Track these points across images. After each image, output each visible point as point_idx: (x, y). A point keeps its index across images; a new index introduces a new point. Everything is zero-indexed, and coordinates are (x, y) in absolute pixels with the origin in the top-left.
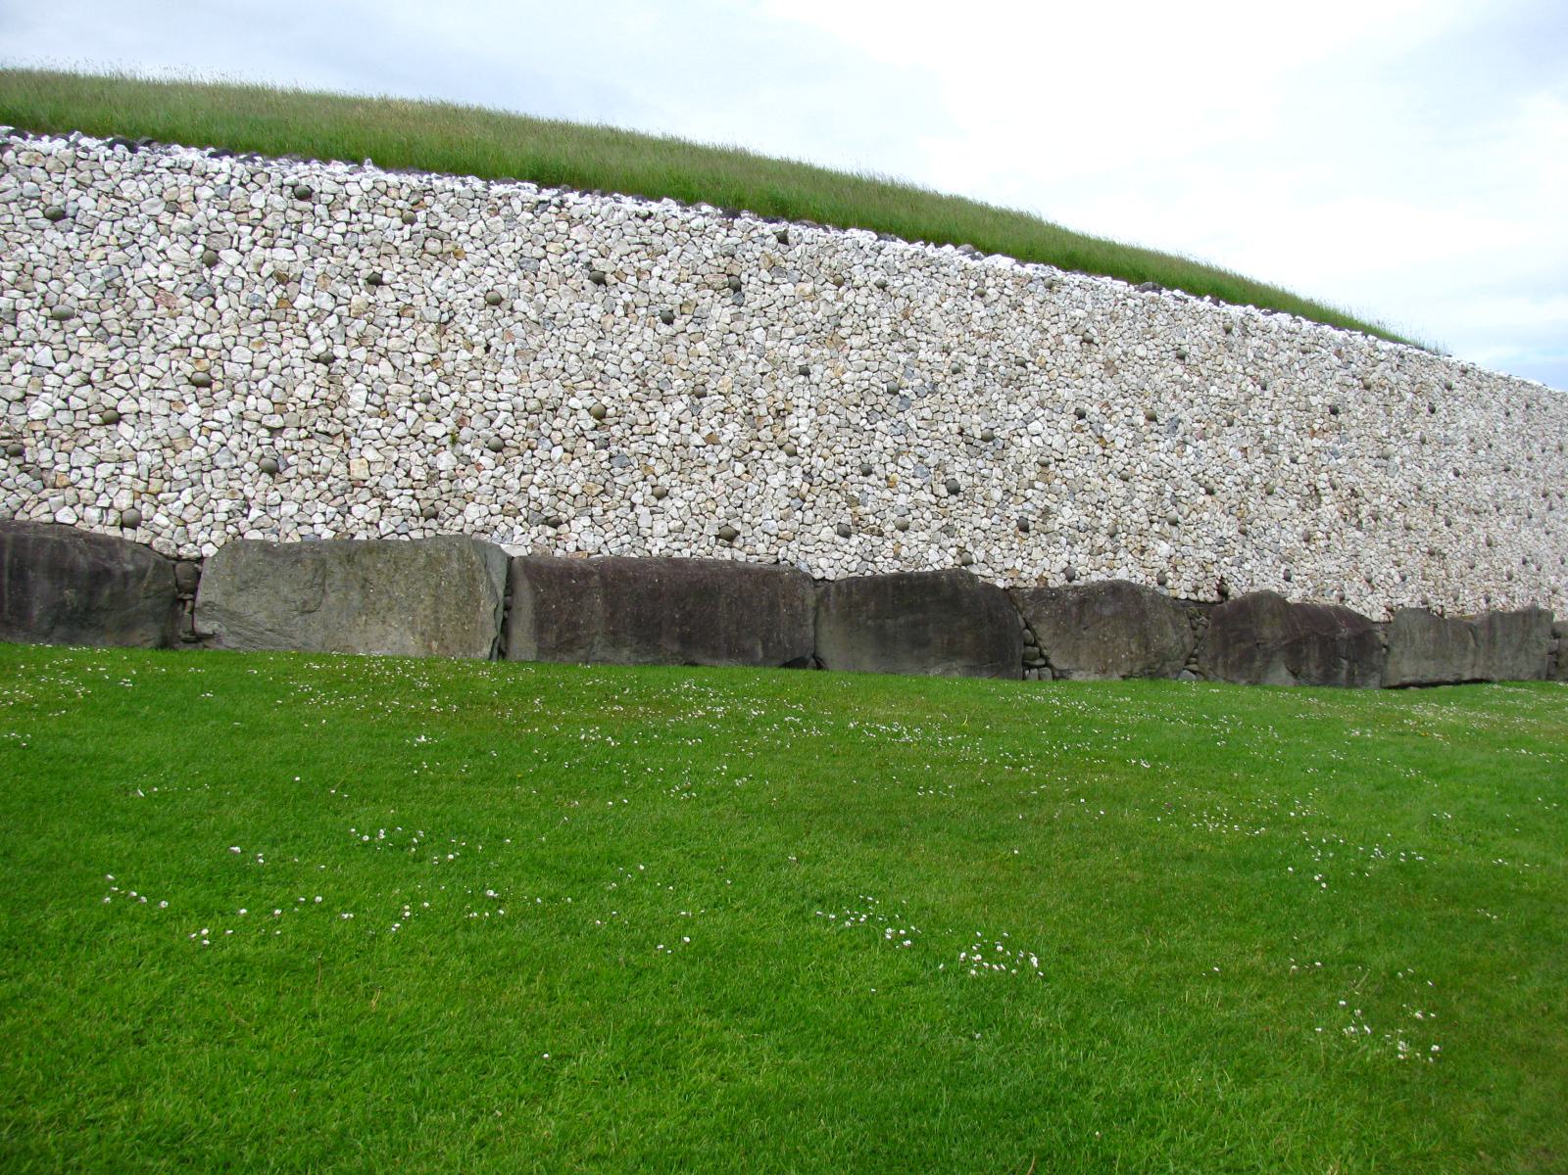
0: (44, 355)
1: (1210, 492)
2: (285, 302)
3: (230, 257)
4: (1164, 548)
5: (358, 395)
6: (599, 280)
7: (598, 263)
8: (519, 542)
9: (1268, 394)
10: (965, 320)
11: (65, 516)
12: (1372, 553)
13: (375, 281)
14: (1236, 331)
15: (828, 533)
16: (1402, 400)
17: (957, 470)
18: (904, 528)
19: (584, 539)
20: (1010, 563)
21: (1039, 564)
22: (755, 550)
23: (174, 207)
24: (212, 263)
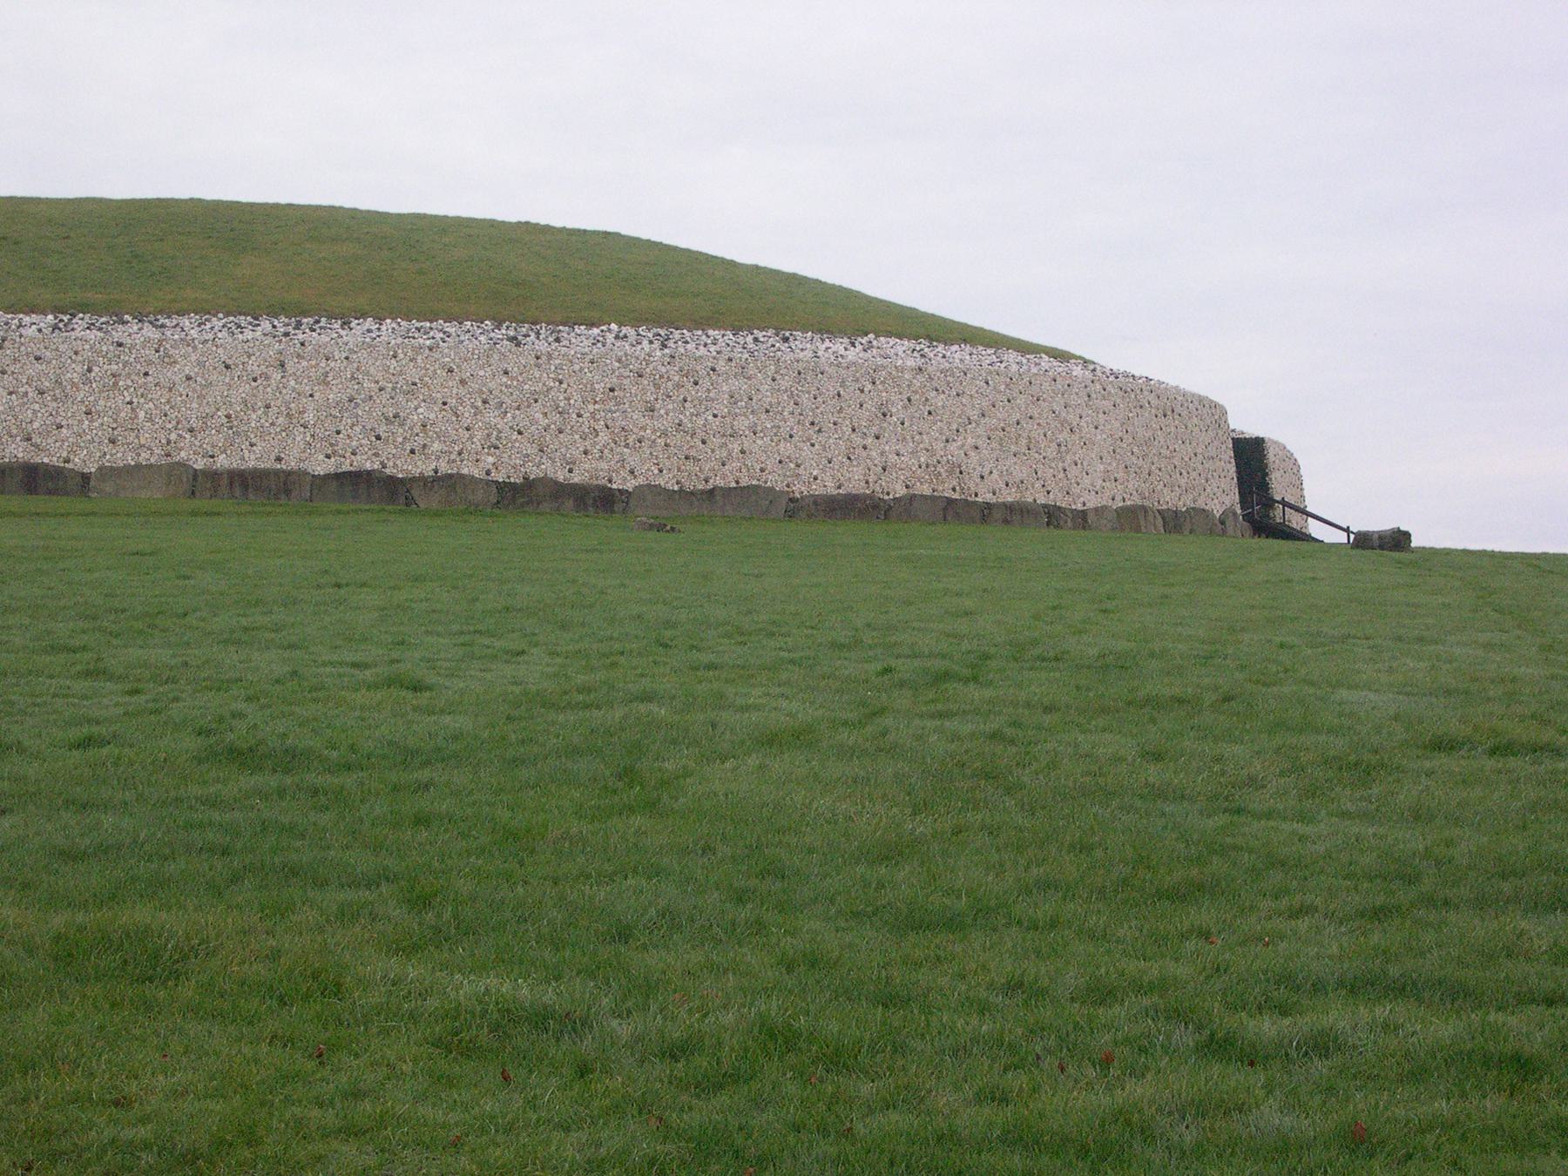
0: (37, 407)
1: (520, 433)
2: (116, 384)
3: (96, 369)
4: (491, 459)
5: (142, 414)
6: (227, 367)
7: (229, 362)
9: (564, 386)
10: (386, 369)
11: (46, 460)
12: (633, 461)
13: (146, 374)
14: (544, 358)
15: (321, 457)
16: (669, 379)
17: (382, 430)
18: (354, 453)
19: (222, 462)
20: (402, 467)
22: (291, 463)
23: (76, 353)
24: (90, 370)
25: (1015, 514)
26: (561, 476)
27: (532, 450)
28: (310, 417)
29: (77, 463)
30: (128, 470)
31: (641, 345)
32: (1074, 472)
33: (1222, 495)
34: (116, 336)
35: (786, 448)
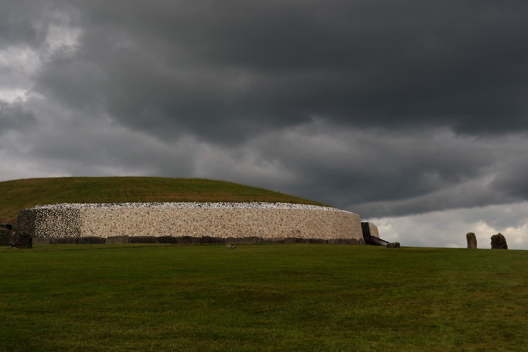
8: (130, 236)
10: (171, 213)
12: (227, 232)
19: (136, 235)
20: (176, 235)
21: (180, 235)
25: (311, 241)
26: (211, 236)
27: (204, 230)
28: (155, 224)
29: (103, 236)
30: (113, 237)
31: (228, 207)
32: (325, 231)
33: (359, 236)
34: (112, 208)
35: (260, 228)
